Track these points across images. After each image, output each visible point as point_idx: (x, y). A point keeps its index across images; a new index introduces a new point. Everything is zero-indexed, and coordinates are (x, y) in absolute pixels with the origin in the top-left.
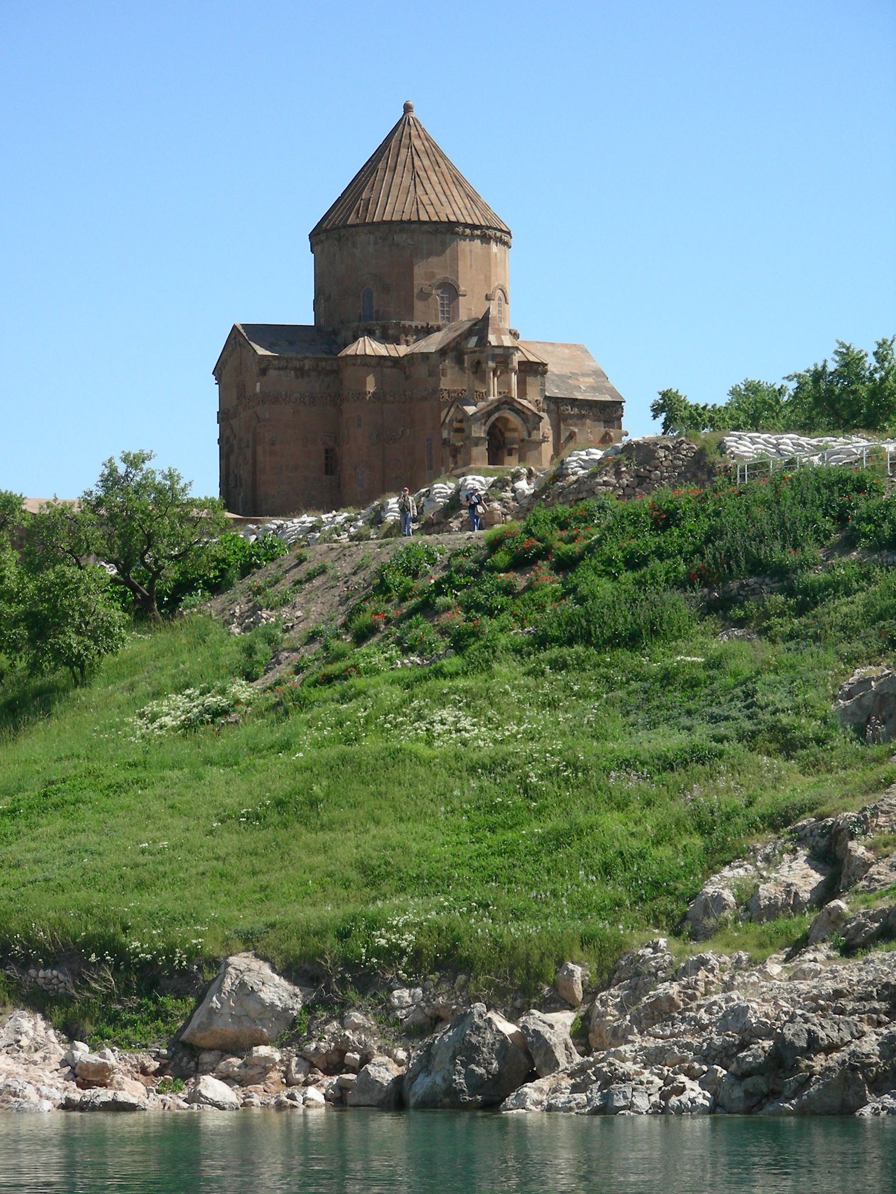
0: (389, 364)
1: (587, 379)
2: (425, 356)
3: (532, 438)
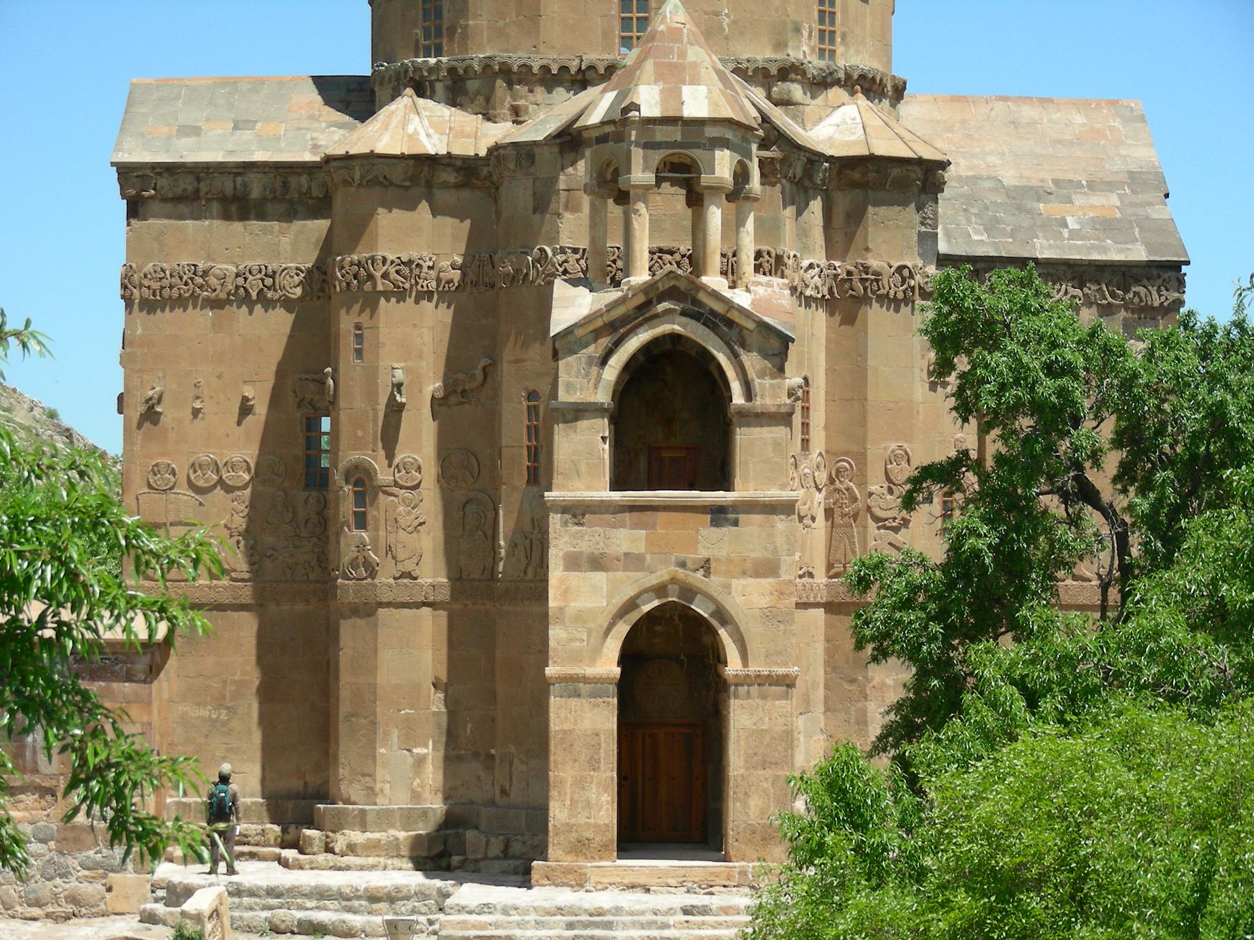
0: (450, 177)
1: (1096, 200)
2: (524, 152)
3: (758, 402)
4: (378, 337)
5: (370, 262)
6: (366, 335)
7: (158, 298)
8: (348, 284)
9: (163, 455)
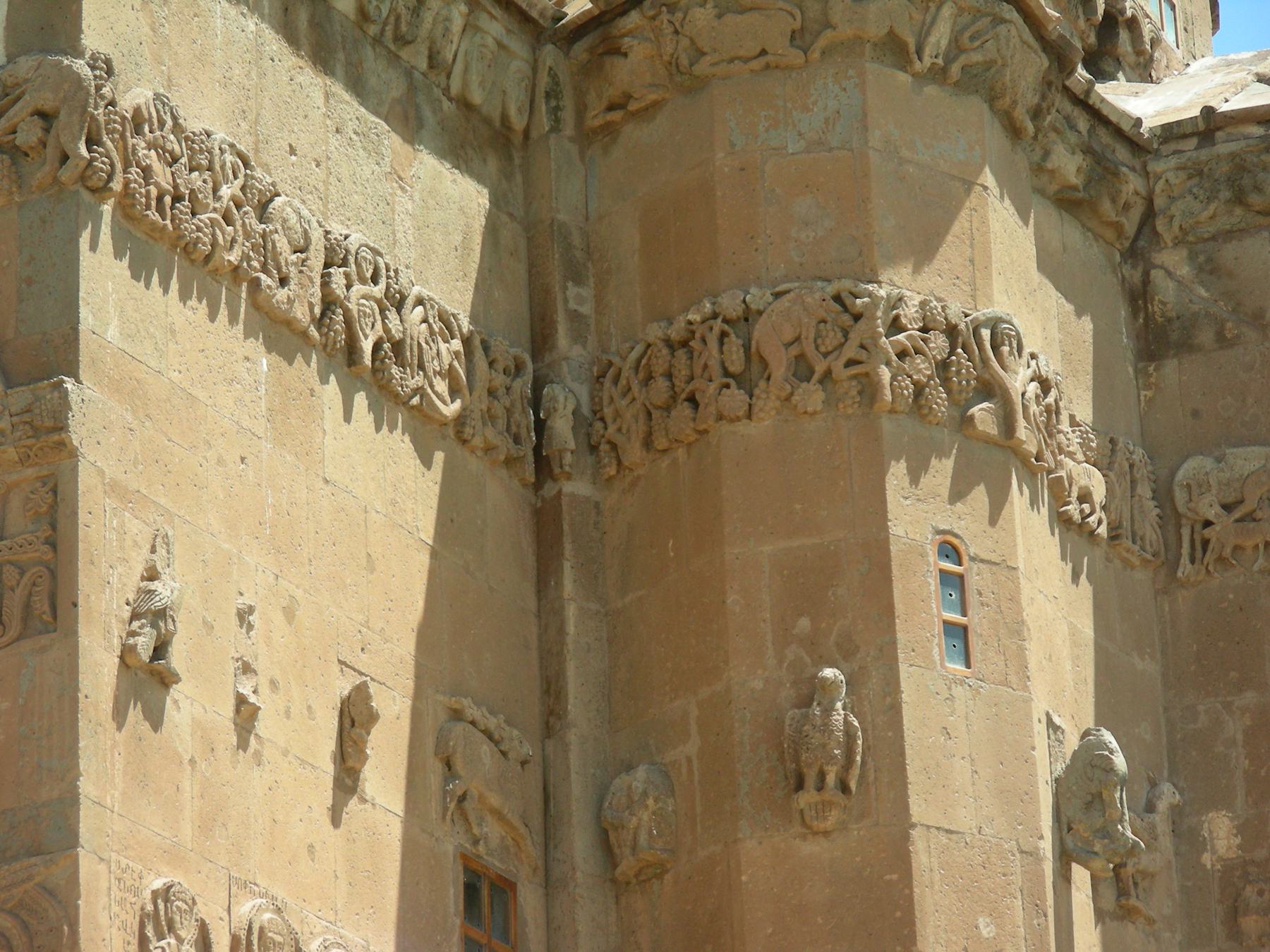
4: (1014, 599)
5: (986, 333)
6: (973, 582)
7: (168, 222)
8: (919, 389)
9: (174, 856)
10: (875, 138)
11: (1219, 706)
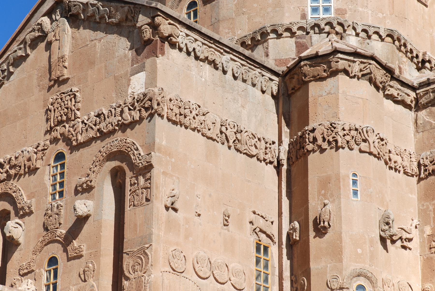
10: (340, 91)
11: (428, 204)
